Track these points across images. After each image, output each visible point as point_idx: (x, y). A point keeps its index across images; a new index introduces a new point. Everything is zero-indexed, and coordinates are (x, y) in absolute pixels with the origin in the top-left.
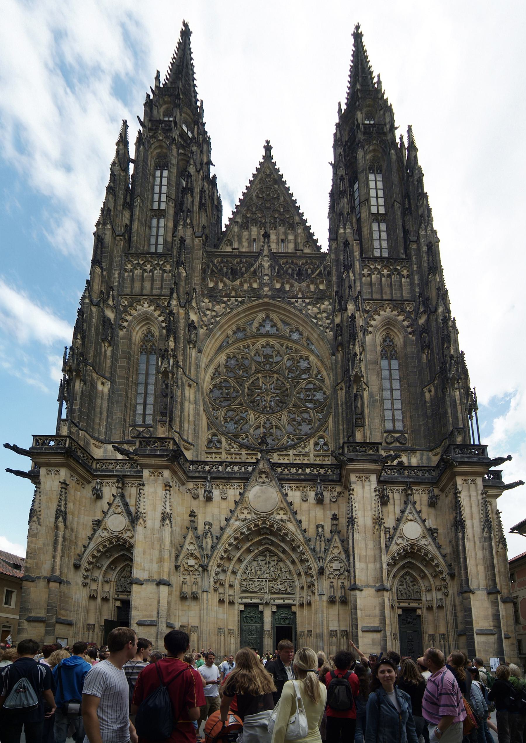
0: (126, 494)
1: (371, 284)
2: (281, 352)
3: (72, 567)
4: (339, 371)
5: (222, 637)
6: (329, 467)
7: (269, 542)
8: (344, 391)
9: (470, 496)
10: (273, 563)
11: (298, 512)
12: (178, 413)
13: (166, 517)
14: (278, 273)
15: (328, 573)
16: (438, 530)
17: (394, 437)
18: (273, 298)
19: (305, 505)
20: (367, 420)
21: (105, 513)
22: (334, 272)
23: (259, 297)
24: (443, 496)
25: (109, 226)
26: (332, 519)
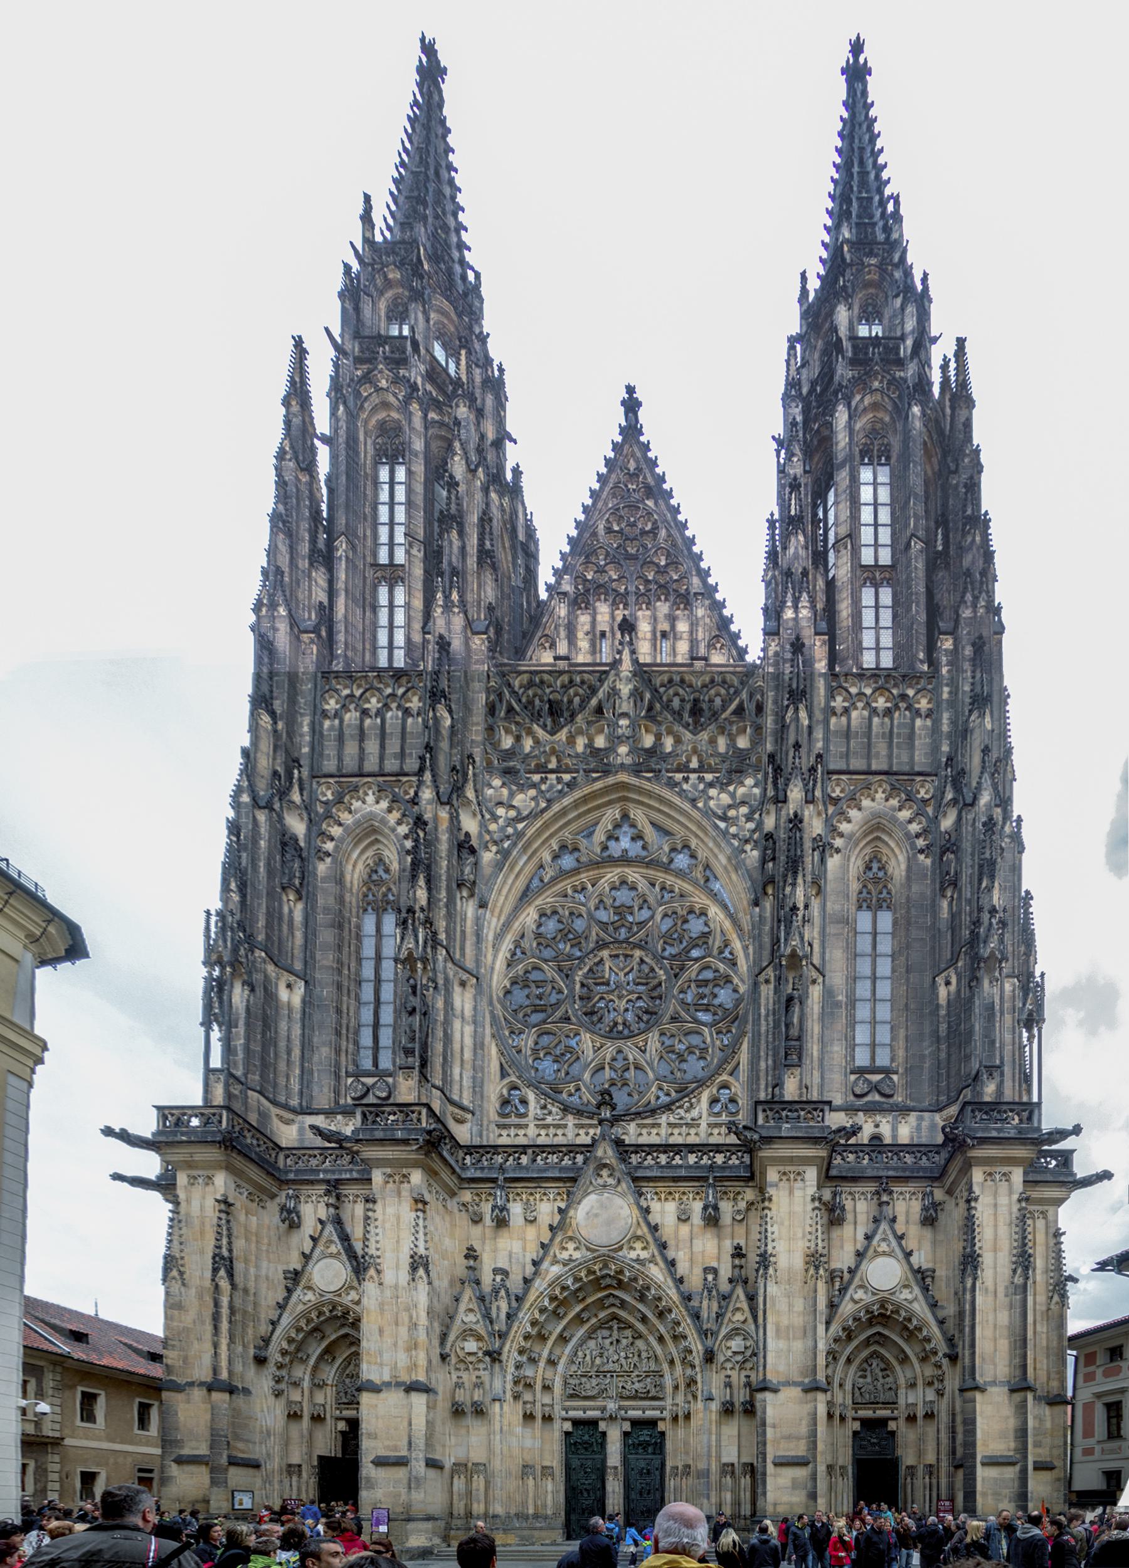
0: (346, 1217)
1: (847, 734)
2: (651, 900)
3: (251, 1360)
4: (767, 940)
5: (531, 1482)
6: (733, 1149)
7: (617, 1302)
8: (772, 986)
9: (995, 1205)
10: (624, 1342)
11: (671, 1243)
12: (439, 1047)
13: (418, 1263)
14: (650, 709)
15: (722, 1358)
16: (934, 1271)
17: (869, 1082)
18: (636, 770)
19: (685, 1229)
20: (815, 1048)
21: (307, 1257)
22: (769, 706)
23: (606, 772)
24: (950, 1205)
25: (282, 611)
26: (733, 1256)
